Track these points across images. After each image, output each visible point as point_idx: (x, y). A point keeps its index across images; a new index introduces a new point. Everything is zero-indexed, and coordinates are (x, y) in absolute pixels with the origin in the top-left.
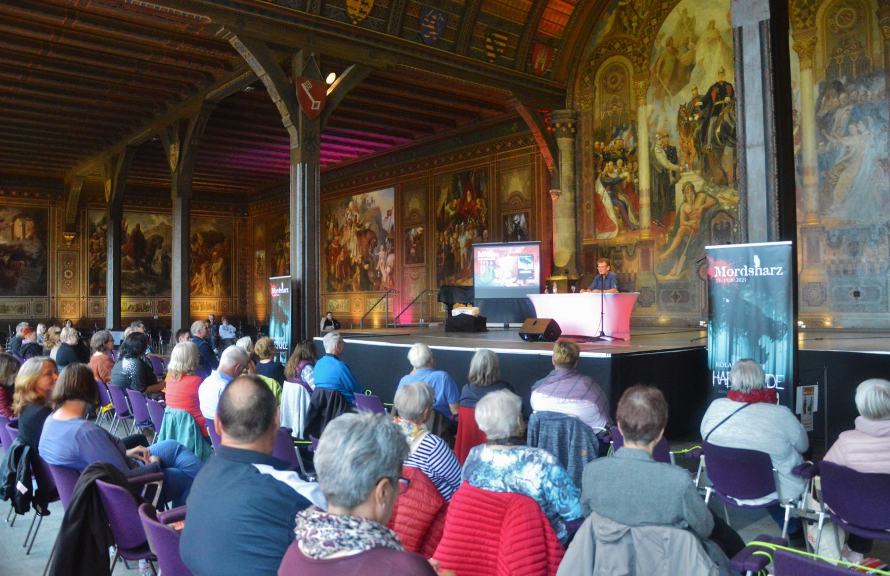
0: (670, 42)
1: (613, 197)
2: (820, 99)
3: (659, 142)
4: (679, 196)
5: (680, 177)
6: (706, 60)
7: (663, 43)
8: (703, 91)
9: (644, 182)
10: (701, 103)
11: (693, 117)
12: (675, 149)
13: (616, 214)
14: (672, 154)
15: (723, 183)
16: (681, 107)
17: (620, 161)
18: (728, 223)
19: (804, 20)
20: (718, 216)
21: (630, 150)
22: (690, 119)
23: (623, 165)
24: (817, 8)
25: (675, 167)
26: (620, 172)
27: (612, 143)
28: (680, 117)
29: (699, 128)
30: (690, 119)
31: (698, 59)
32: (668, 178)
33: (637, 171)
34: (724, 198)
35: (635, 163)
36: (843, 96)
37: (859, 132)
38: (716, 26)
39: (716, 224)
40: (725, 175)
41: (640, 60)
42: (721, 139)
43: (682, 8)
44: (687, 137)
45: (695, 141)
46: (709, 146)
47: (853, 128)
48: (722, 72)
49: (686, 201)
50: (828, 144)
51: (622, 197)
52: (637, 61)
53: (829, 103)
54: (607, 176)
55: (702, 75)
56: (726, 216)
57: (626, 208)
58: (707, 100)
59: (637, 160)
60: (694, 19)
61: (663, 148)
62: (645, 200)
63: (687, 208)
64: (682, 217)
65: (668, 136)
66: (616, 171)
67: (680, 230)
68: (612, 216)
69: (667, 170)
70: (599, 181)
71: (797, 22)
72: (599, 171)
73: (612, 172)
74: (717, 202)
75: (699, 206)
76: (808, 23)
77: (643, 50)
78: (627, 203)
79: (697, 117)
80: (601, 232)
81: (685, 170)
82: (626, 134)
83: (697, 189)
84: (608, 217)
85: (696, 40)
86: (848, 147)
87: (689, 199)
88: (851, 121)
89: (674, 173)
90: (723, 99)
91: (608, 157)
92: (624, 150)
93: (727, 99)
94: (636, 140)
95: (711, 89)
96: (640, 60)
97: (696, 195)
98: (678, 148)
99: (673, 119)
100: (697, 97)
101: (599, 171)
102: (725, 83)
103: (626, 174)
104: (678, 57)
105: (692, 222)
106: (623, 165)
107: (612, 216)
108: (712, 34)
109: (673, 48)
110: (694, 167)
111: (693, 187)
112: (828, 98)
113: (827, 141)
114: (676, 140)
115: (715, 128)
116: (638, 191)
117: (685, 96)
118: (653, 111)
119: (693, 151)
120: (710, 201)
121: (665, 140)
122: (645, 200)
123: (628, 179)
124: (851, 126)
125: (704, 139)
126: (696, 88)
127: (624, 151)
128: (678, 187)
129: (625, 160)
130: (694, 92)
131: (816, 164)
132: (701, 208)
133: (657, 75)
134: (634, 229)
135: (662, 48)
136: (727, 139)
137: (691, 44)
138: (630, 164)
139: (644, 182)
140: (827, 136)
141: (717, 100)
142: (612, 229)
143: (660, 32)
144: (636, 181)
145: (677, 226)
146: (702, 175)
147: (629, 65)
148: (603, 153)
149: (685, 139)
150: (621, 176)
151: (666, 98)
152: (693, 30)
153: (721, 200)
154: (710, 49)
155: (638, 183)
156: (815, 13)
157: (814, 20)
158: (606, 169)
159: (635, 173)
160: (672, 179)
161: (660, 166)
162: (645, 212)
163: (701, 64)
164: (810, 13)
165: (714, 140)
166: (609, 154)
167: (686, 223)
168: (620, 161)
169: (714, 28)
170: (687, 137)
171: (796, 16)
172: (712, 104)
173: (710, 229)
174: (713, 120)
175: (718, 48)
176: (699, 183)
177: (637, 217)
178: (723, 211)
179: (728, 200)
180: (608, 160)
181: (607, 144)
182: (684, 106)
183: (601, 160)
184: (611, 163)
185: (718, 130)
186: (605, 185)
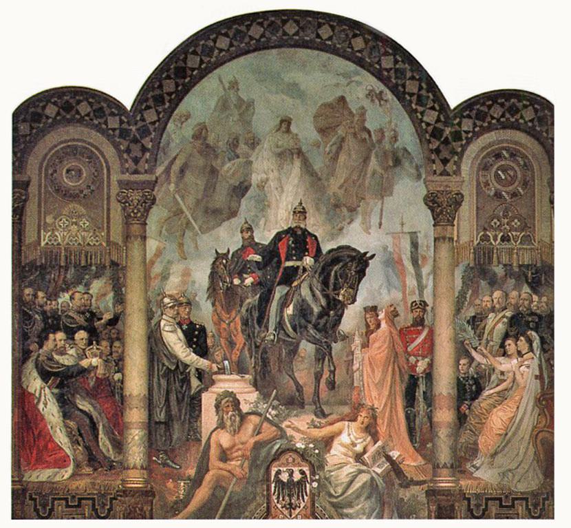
0: (201, 134)
1: (64, 403)
2: (462, 295)
3: (171, 313)
4: (209, 418)
5: (213, 383)
6: (272, 184)
7: (188, 130)
8: (264, 236)
9: (135, 382)
10: (258, 258)
11: (243, 280)
12: (203, 330)
13: (70, 434)
14: (196, 337)
15: (294, 402)
16: (219, 257)
17: (81, 335)
18: (302, 473)
19: (445, 162)
20: (283, 459)
21: (107, 316)
22: (236, 281)
23: (90, 343)
24: (464, 148)
25: (203, 363)
26: (83, 355)
27: (65, 297)
28: (213, 276)
29: (252, 300)
30: (236, 281)
31: (255, 179)
32: (186, 381)
33: (121, 359)
34: (298, 430)
35: (117, 344)
36: (497, 294)
37: (520, 354)
38: (293, 128)
39: (279, 473)
40: (299, 388)
41: (136, 149)
42: (294, 329)
43: (230, 78)
44: (229, 312)
45: (245, 323)
46: (271, 334)
47: (511, 345)
48: (301, 212)
49: (221, 425)
50: (474, 365)
51: (84, 405)
52: (128, 151)
53: (477, 302)
54: (51, 359)
55: (263, 205)
56: (299, 460)
57: (94, 426)
58: (271, 254)
59: (120, 337)
60: (250, 104)
61: (180, 324)
62: (135, 416)
63: (225, 439)
64: (214, 452)
65: (189, 303)
66: (72, 352)
67: (208, 477)
68: (61, 438)
69: (186, 366)
70: (30, 365)
71: (434, 162)
72: (34, 347)
73: (62, 352)
74: (283, 434)
75: (247, 435)
76: (450, 167)
77: (145, 132)
78: (95, 414)
79: (249, 281)
80: (34, 468)
81: (222, 371)
82: (97, 286)
83: (245, 408)
84: (51, 440)
85: (254, 143)
86: (502, 373)
87: (228, 423)
88: (506, 336)
89: (200, 374)
90: (300, 259)
91: (53, 323)
92: (93, 314)
93: (308, 261)
94: (120, 299)
95: (278, 237)
96: (136, 149)
97: (243, 417)
98: (210, 328)
99: (201, 275)
100: (250, 245)
101: (34, 347)
102: (305, 231)
103: (95, 361)
104: (217, 163)
105: (234, 464)
106: (90, 343)
107: (61, 438)
108: (286, 142)
109: (208, 146)
110: (240, 369)
111: (236, 404)
112: (476, 293)
113: (472, 359)
114: (205, 313)
115: (284, 304)
116: (122, 397)
117: (228, 239)
118: (159, 253)
119: (240, 339)
120: (268, 431)
121: (184, 312)
122: (135, 416)
123: (100, 371)
124: (508, 342)
125: (262, 319)
126: (250, 229)
127: (93, 316)
128: (208, 400)
129: (94, 336)
130: (247, 235)
131: (454, 392)
132: (252, 441)
133: (172, 187)
134: (112, 467)
135: (183, 139)
136: (306, 327)
137: (243, 148)
138: (104, 343)
139: (135, 382)
140: (474, 354)
141: (288, 259)
142: (62, 463)
143: (182, 108)
144: (117, 376)
145: (203, 469)
146: (255, 384)
147: (110, 151)
148: (44, 313)
149: (224, 315)
150: (85, 363)
151: (188, 234)
152: (249, 123)
153: (289, 432)
154: (280, 167)
155: (122, 382)
156: (461, 155)
157: (458, 164)
158: (49, 345)
159: (119, 363)
160: (195, 383)
161: (172, 356)
162: (136, 437)
163: (261, 186)
164: (454, 153)
165: (280, 325)
166: (56, 316)
167: (222, 465)
168: (81, 335)
169: (288, 131)
170: (229, 312)
171: (432, 151)
172: (279, 262)
173: (268, 479)
174: (279, 292)
175: (296, 167)
176: (249, 398)
177: (119, 446)
178: (296, 451)
179: (303, 433)
180: (56, 329)
181: (53, 296)
182: (226, 255)
183: (39, 326)
184: (60, 335)
185: (290, 311)
186: (45, 375)
